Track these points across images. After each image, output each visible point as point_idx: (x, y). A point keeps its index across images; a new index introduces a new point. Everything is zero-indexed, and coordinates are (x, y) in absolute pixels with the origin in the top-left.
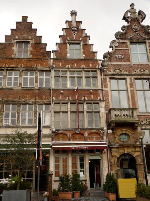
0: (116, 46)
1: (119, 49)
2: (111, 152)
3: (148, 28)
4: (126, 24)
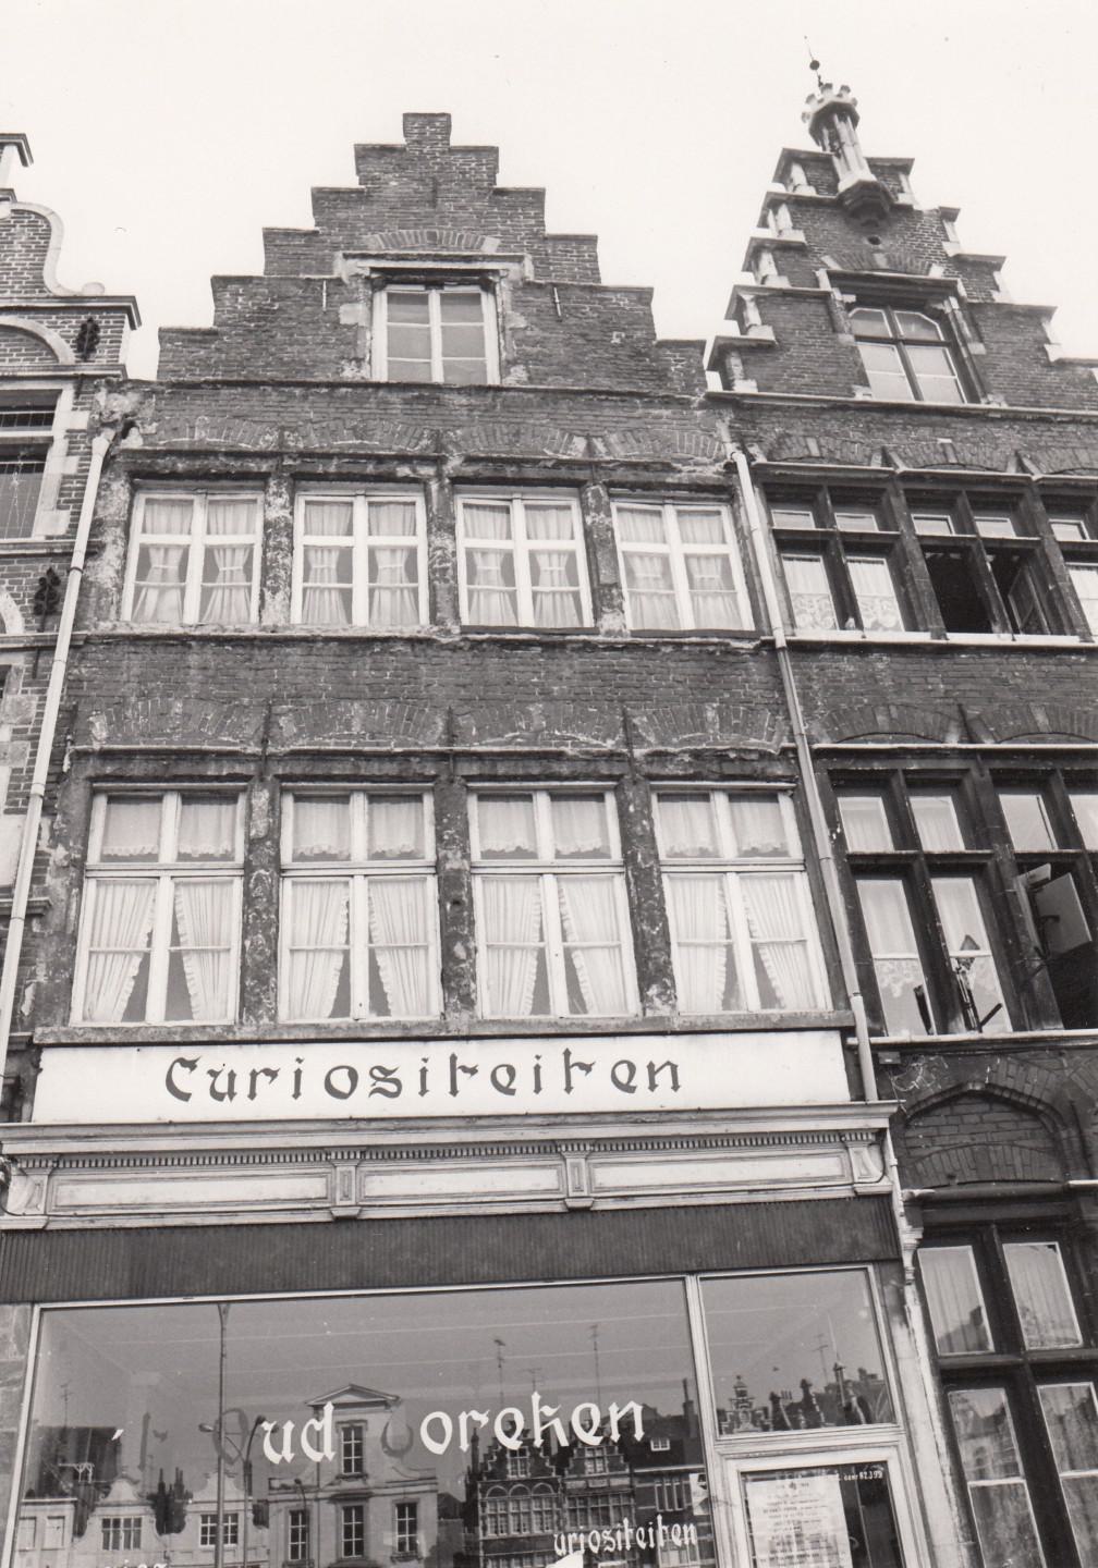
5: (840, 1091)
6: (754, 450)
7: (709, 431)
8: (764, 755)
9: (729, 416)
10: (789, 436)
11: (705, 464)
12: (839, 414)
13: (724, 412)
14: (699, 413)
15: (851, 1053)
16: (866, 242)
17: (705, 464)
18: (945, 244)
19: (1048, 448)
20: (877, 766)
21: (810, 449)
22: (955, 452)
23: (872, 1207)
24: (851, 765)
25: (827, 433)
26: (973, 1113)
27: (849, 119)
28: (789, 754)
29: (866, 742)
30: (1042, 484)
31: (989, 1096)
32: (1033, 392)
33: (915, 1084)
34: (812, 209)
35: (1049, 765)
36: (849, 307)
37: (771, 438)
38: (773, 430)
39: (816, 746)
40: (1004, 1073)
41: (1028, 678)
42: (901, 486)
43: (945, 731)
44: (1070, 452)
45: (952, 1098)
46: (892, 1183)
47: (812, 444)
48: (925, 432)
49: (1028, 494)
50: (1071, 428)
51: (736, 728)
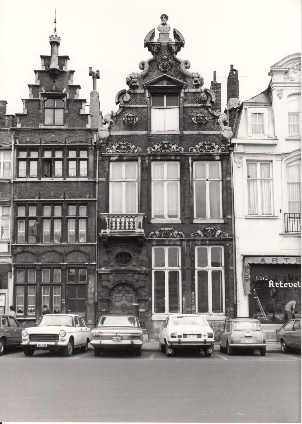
0: (125, 100)
1: (131, 106)
2: (101, 281)
3: (187, 66)
4: (148, 56)
5: (6, 251)
6: (17, 141)
7: (10, 137)
8: (6, 202)
9: (14, 133)
10: (24, 137)
11: (8, 144)
12: (34, 131)
13: (13, 132)
14: (9, 132)
15: (9, 246)
16: (52, 82)
17: (8, 144)
18: (69, 81)
19: (72, 136)
20: (23, 203)
21: (28, 140)
22: (54, 139)
23: (9, 265)
24: (19, 203)
25: (32, 136)
26: (26, 254)
27: (56, 45)
28: (10, 201)
29: (22, 199)
30: (68, 146)
31: (28, 252)
32: (74, 122)
33: (18, 250)
34: (43, 73)
35: (51, 202)
36: (45, 101)
37: (20, 138)
38: (21, 135)
39: (14, 200)
40: (30, 249)
41: (53, 187)
42: (42, 147)
43: (36, 197)
44: (76, 137)
45: (23, 252)
46: (12, 263)
47: (28, 138)
48: (50, 134)
49: (65, 148)
50: (78, 131)
51: (3, 197)
